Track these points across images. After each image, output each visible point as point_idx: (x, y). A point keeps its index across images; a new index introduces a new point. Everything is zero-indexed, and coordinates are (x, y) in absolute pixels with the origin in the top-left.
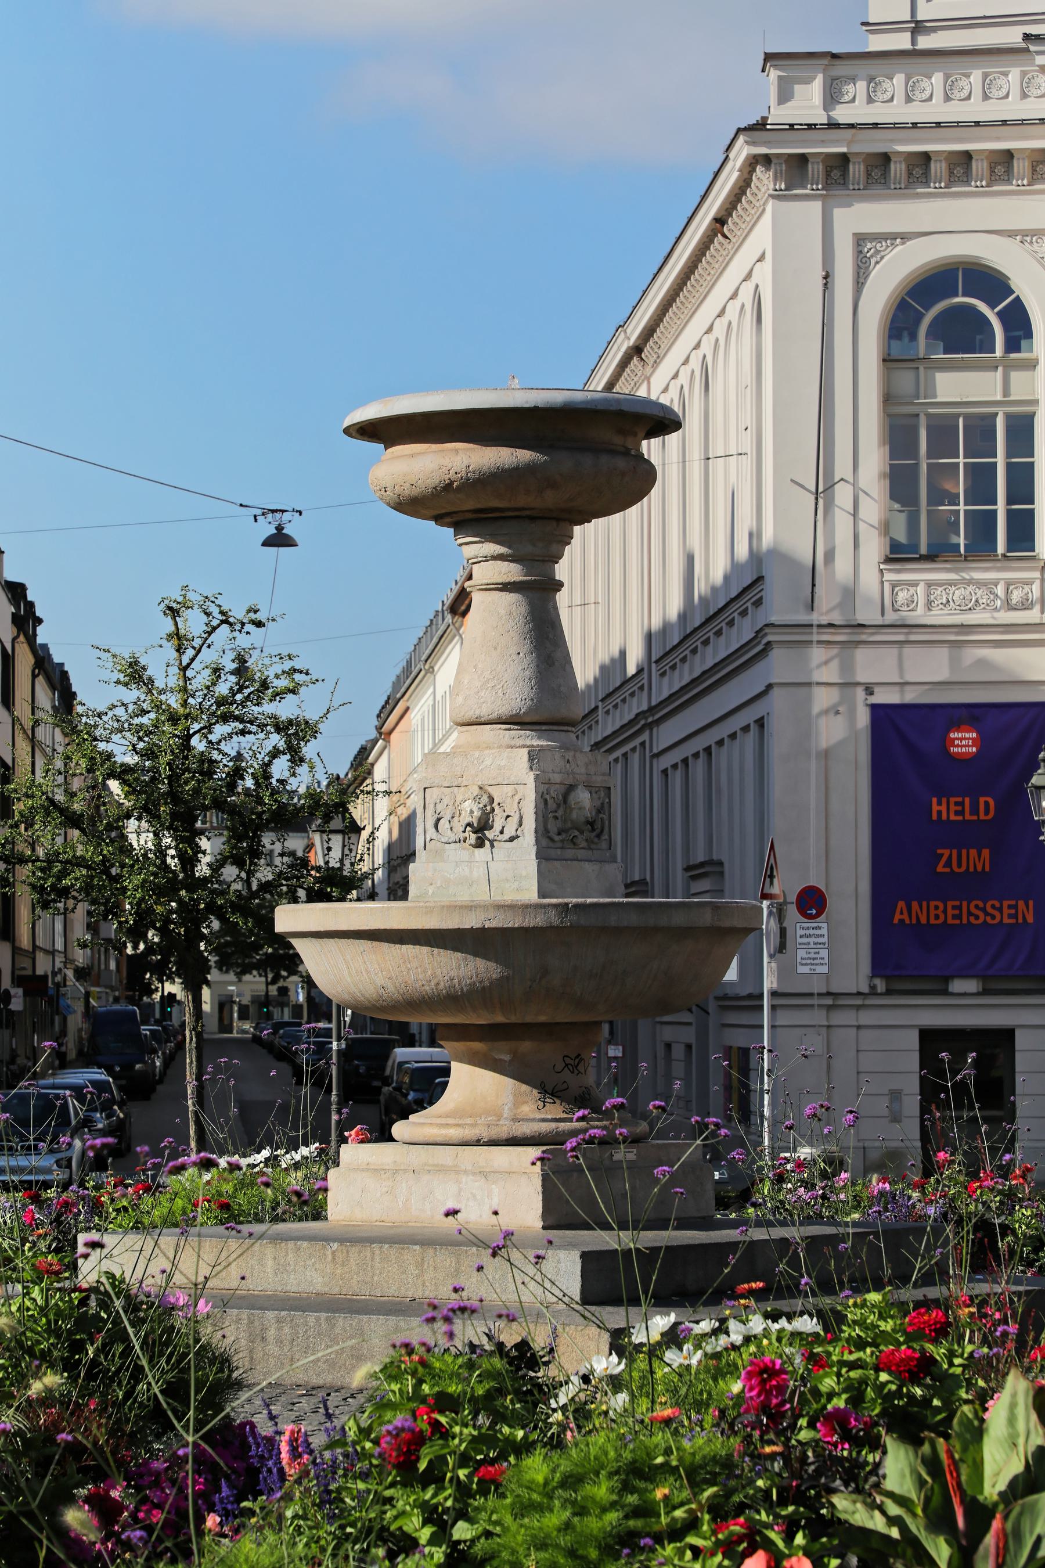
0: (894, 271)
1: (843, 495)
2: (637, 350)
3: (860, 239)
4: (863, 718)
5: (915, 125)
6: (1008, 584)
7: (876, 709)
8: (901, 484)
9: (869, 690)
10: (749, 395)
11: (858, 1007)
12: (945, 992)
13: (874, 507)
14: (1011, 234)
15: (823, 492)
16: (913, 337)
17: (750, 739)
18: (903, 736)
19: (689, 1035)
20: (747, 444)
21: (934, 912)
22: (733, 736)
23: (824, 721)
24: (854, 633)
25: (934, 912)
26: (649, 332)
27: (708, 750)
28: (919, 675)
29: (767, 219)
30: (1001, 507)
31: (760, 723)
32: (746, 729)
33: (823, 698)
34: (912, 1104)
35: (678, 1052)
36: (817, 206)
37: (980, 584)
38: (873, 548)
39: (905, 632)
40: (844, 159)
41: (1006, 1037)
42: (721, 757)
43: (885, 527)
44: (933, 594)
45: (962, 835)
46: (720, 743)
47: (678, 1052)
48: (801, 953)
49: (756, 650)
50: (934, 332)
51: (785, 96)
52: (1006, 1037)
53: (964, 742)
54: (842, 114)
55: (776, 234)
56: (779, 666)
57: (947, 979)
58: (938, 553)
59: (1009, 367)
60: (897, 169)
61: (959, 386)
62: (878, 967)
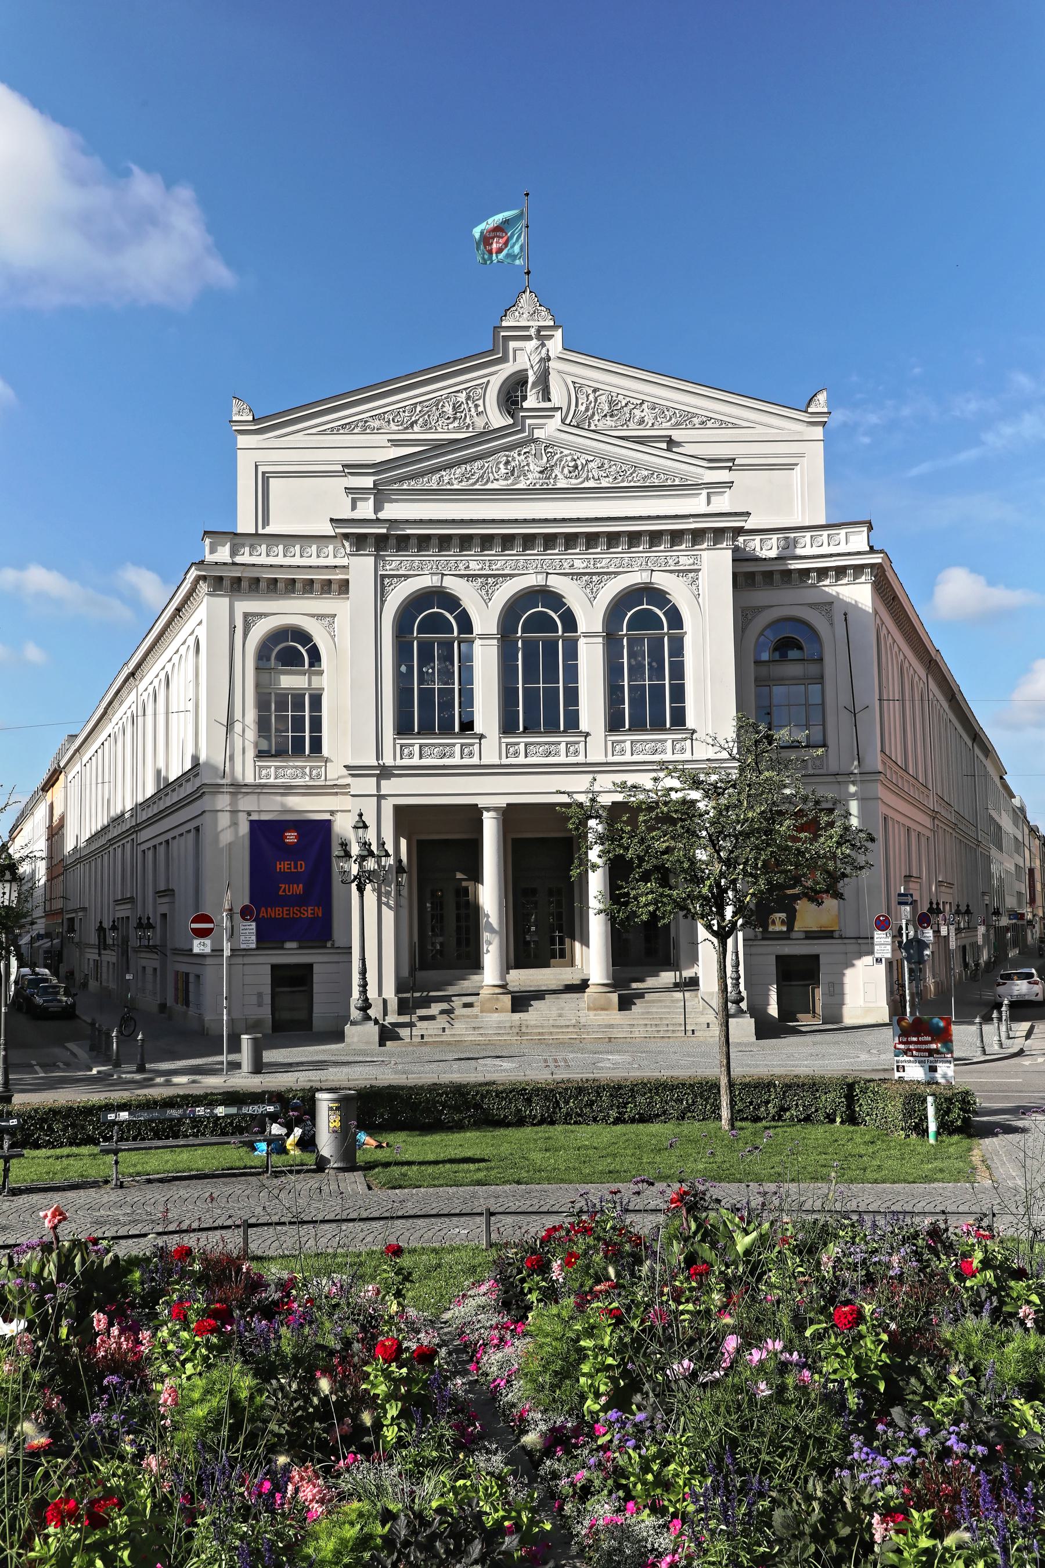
0: (260, 630)
1: (238, 727)
2: (132, 674)
3: (246, 615)
4: (244, 829)
5: (271, 566)
6: (311, 768)
7: (252, 823)
8: (263, 725)
9: (249, 813)
10: (192, 686)
11: (243, 956)
12: (282, 948)
13: (251, 735)
14: (313, 616)
15: (229, 726)
16: (269, 659)
17: (191, 836)
18: (266, 834)
19: (157, 964)
20: (190, 706)
21: (278, 912)
22: (181, 835)
23: (229, 829)
24: (238, 788)
25: (278, 912)
26: (139, 666)
27: (167, 842)
28: (270, 808)
29: (203, 608)
30: (307, 734)
31: (197, 829)
32: (189, 831)
33: (224, 820)
34: (267, 999)
35: (149, 971)
36: (227, 600)
37: (296, 767)
38: (251, 753)
39: (259, 789)
40: (239, 579)
41: (309, 967)
42: (174, 845)
43: (256, 745)
44: (273, 772)
45: (291, 878)
46: (174, 838)
47: (149, 971)
48: (242, 938)
49: (198, 795)
50: (277, 658)
51: (213, 551)
52: (309, 967)
53: (291, 837)
54: (238, 559)
55: (208, 613)
56: (205, 803)
57: (284, 941)
58: (280, 753)
59: (312, 674)
60: (263, 585)
61: (290, 681)
62: (258, 940)
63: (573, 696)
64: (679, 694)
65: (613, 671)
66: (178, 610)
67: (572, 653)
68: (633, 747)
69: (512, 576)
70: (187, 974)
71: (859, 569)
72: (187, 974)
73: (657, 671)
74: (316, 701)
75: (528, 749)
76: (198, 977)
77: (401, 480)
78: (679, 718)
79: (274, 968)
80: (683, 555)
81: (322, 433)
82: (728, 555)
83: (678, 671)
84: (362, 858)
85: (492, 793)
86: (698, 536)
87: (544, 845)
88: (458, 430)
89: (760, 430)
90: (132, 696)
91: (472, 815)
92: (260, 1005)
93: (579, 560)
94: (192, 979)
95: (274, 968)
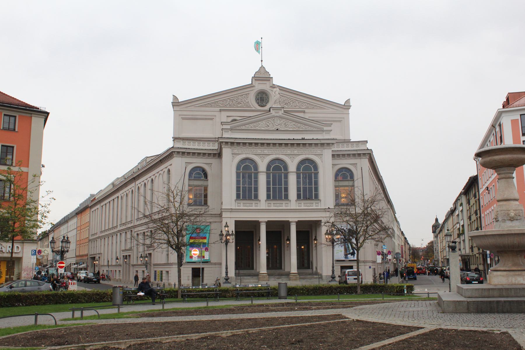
2: (134, 178)
63: (286, 190)
64: (316, 189)
65: (298, 183)
66: (161, 160)
67: (286, 177)
68: (304, 205)
69: (270, 155)
70: (162, 271)
71: (364, 154)
72: (162, 271)
73: (310, 183)
74: (206, 189)
75: (274, 205)
76: (168, 272)
77: (238, 126)
78: (317, 197)
79: (193, 269)
80: (318, 151)
81: (198, 107)
82: (330, 151)
83: (316, 183)
84: (227, 235)
85: (263, 218)
86: (322, 144)
87: (277, 232)
88: (240, 107)
89: (330, 110)
90: (133, 185)
91: (256, 224)
92: (188, 280)
93: (289, 151)
94: (164, 272)
95: (193, 269)
